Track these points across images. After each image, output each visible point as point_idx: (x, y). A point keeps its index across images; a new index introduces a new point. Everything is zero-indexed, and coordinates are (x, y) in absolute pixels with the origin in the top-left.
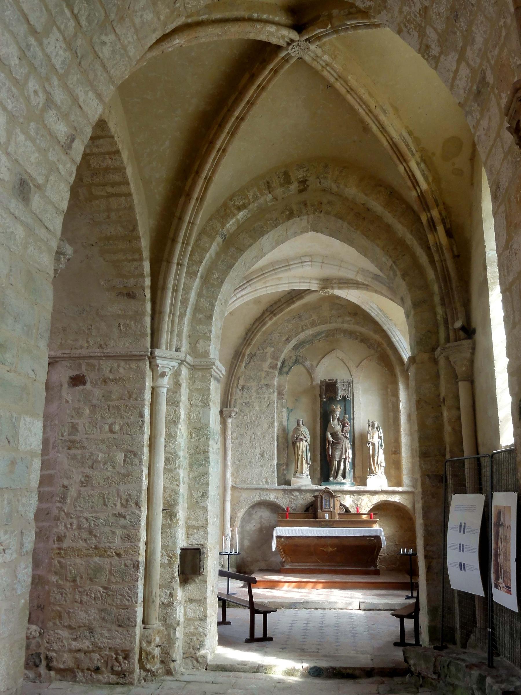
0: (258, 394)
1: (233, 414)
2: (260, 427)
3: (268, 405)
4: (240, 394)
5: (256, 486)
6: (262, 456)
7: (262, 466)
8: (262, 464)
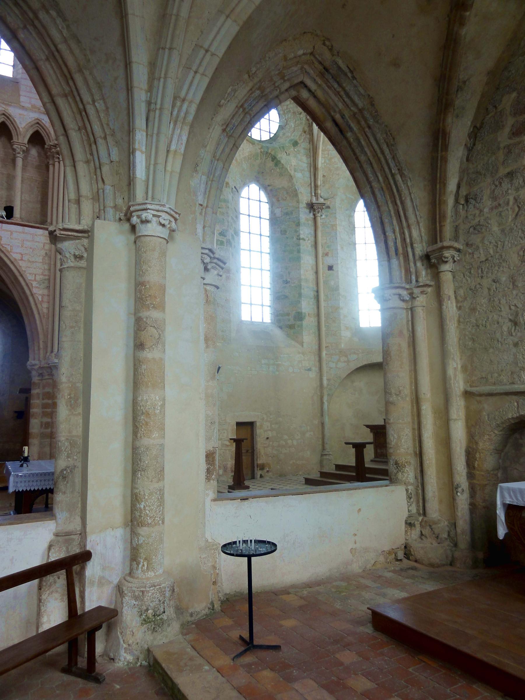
0: (494, 198)
1: (447, 254)
2: (504, 264)
3: (517, 215)
4: (463, 213)
5: (508, 388)
6: (515, 323)
7: (516, 345)
8: (516, 340)
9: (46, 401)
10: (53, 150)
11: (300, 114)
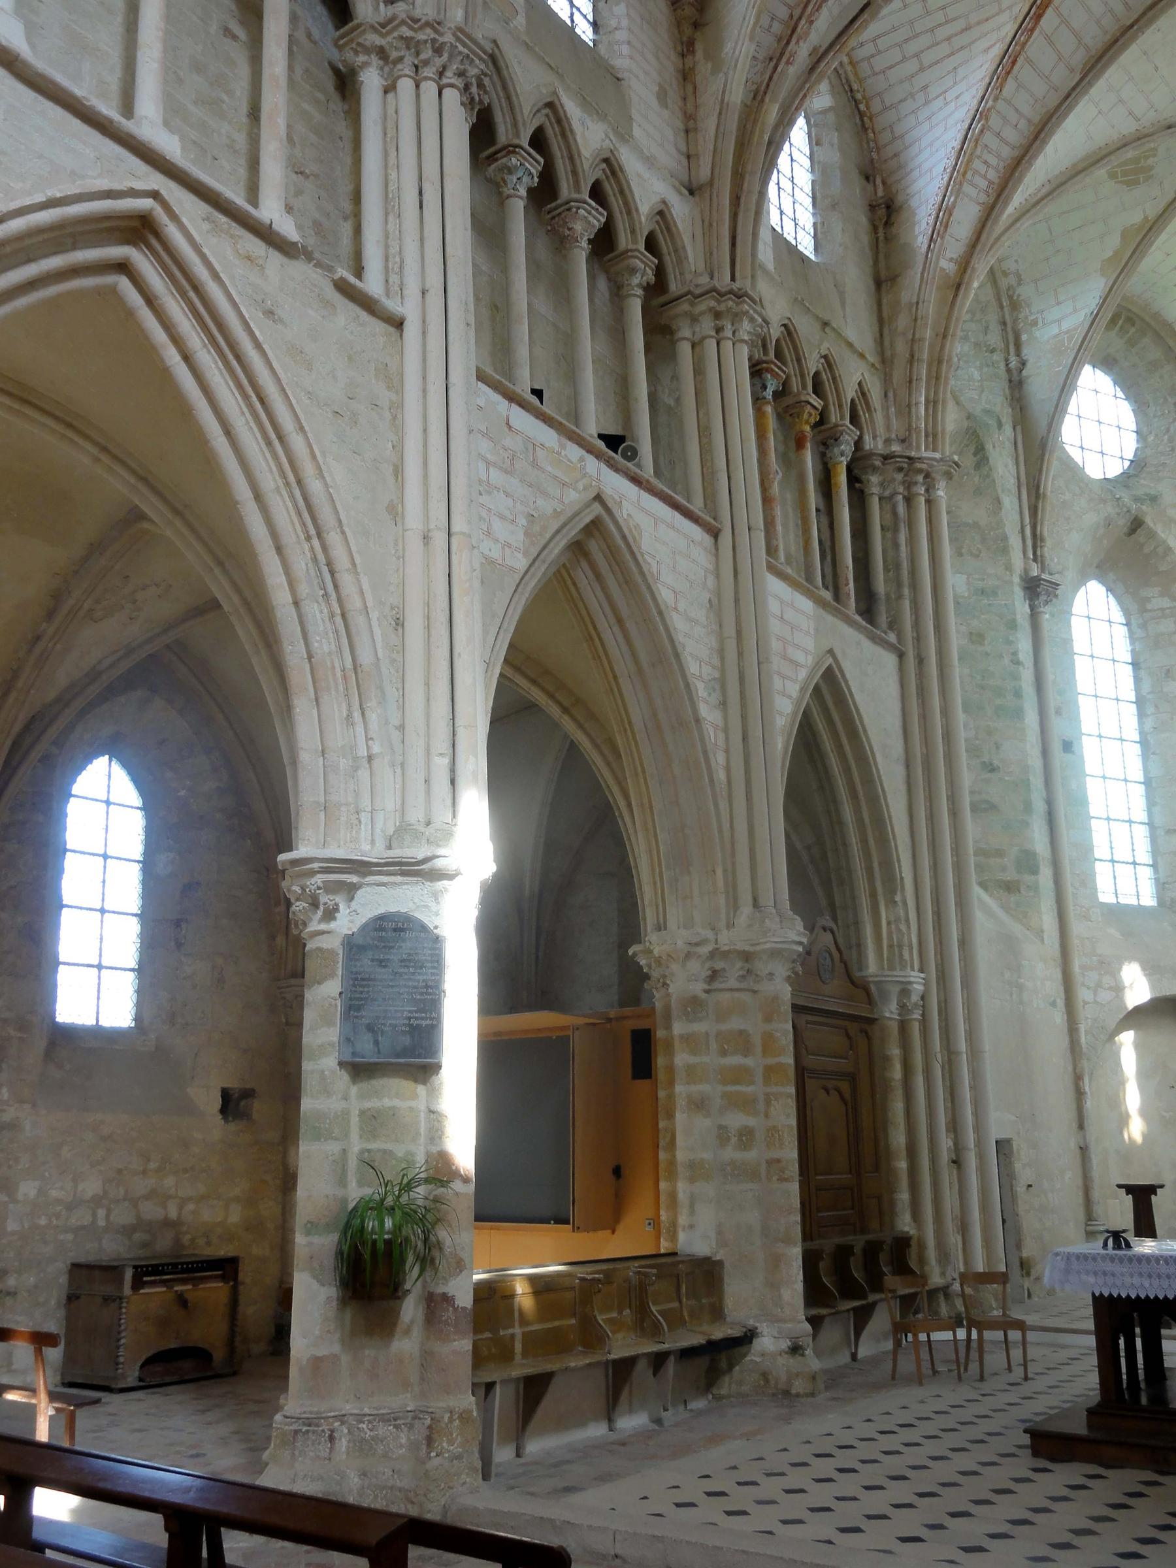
9: (735, 1060)
10: (713, 303)
11: (993, 351)
